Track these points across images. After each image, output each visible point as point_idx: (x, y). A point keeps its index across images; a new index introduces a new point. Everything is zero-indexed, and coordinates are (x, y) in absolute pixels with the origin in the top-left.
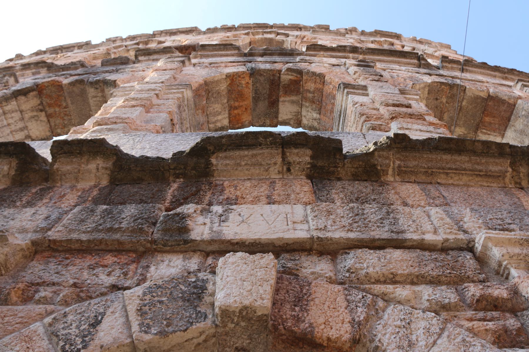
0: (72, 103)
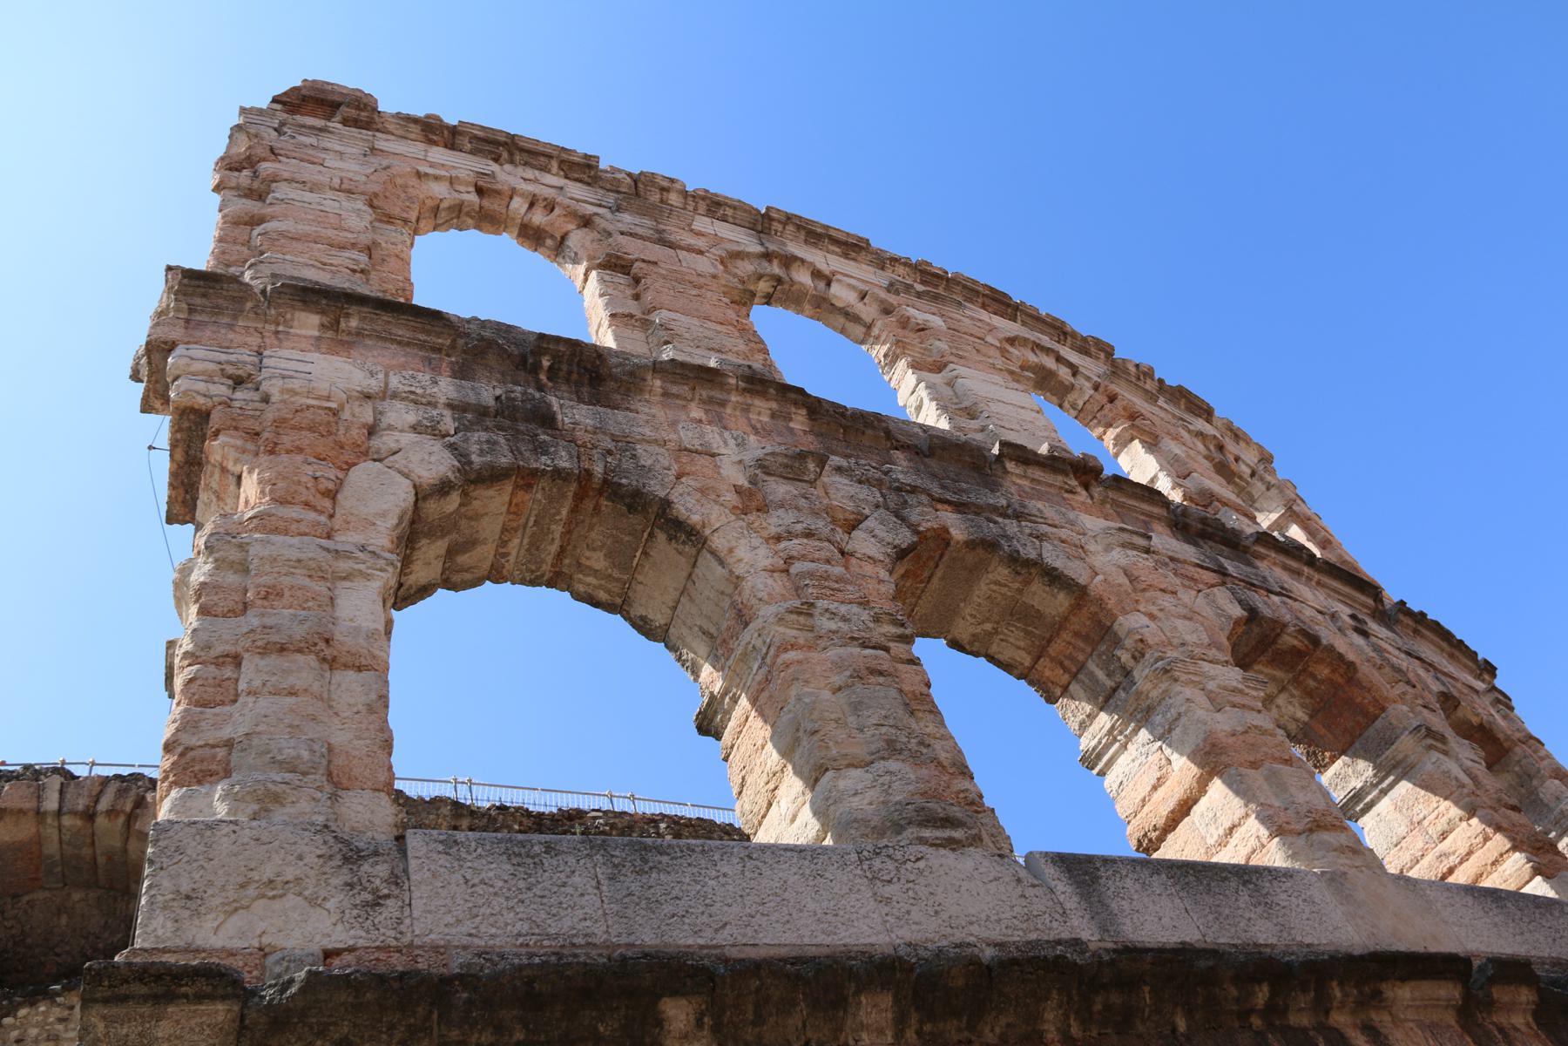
0: (942, 578)
